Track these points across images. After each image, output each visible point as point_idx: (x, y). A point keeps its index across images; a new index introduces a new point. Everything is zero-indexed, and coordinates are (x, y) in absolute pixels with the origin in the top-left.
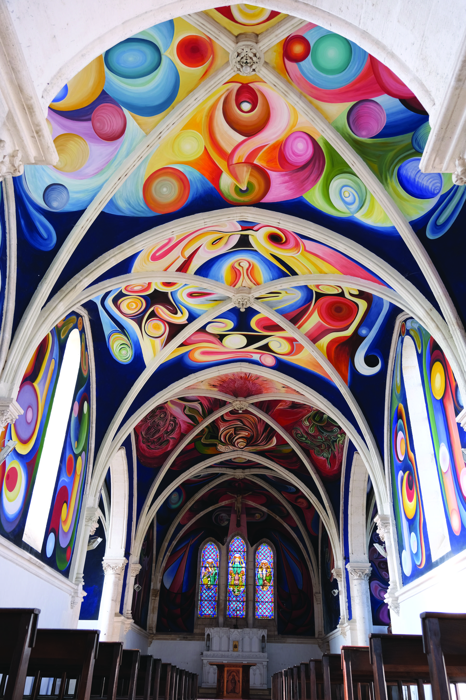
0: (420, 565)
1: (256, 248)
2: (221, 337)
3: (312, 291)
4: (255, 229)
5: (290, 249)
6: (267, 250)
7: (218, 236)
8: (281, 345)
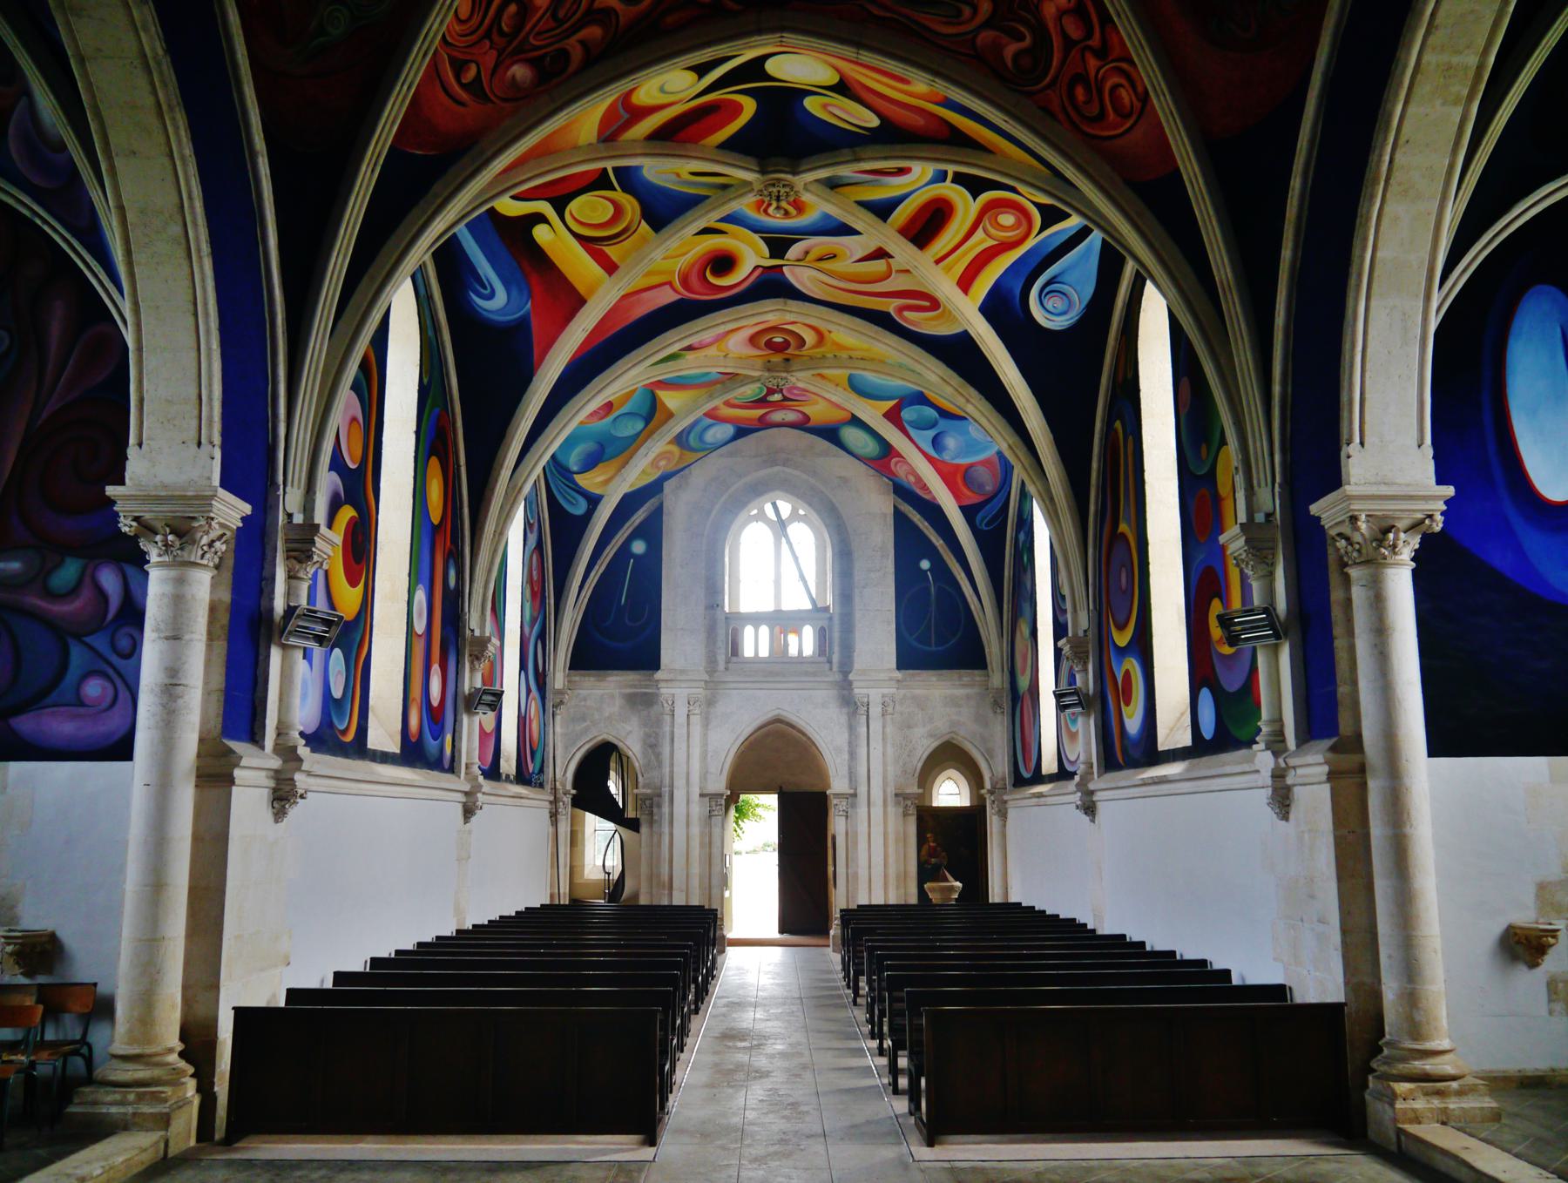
0: (345, 732)
1: (756, 237)
2: (843, 88)
3: (624, 190)
4: (759, 271)
5: (693, 265)
6: (735, 237)
7: (823, 265)
8: (662, 90)
